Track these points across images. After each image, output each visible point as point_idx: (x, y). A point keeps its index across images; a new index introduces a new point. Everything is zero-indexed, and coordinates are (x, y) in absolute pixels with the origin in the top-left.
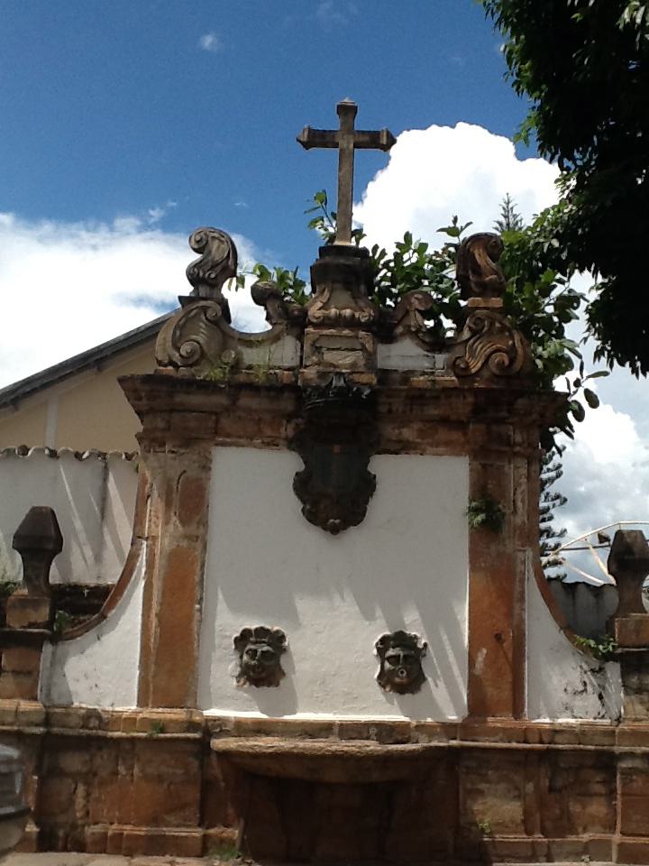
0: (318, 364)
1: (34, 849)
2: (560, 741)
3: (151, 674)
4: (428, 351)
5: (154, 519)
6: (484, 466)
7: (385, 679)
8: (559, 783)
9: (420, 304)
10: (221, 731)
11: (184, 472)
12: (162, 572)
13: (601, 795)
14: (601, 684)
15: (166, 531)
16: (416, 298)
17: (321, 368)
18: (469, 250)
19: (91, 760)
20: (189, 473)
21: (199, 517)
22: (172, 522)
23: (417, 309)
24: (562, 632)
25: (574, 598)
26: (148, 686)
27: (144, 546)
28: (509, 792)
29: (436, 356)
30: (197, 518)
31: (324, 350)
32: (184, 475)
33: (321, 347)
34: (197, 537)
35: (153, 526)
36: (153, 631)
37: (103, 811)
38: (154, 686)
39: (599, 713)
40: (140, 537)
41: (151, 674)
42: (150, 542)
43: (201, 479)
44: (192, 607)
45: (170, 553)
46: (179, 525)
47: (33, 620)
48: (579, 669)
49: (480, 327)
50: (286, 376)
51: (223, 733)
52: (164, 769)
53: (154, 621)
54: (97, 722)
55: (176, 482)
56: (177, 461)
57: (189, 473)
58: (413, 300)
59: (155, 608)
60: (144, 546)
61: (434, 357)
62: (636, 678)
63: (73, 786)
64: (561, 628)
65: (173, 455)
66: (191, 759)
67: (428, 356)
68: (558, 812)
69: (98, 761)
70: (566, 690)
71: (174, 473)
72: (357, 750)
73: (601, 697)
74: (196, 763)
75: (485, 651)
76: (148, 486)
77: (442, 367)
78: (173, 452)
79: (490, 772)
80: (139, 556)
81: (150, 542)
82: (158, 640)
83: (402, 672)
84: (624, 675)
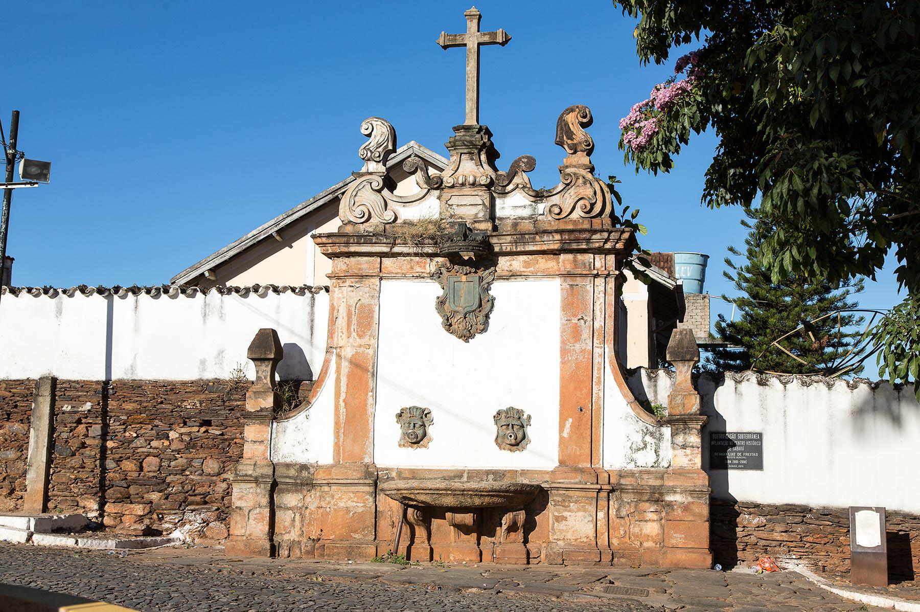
2: (624, 483)
3: (341, 440)
5: (340, 334)
7: (499, 441)
8: (624, 513)
10: (388, 478)
16: (523, 162)
20: (363, 301)
24: (629, 405)
30: (369, 333)
31: (454, 207)
32: (360, 302)
34: (369, 345)
35: (340, 338)
36: (341, 411)
41: (341, 440)
42: (338, 350)
48: (641, 432)
49: (569, 181)
50: (432, 229)
52: (350, 504)
53: (342, 404)
56: (354, 293)
57: (363, 301)
59: (343, 396)
62: (682, 437)
63: (293, 515)
65: (352, 288)
66: (368, 497)
68: (622, 532)
69: (308, 499)
74: (371, 500)
75: (571, 420)
76: (336, 311)
79: (572, 504)
82: (345, 417)
83: (511, 436)
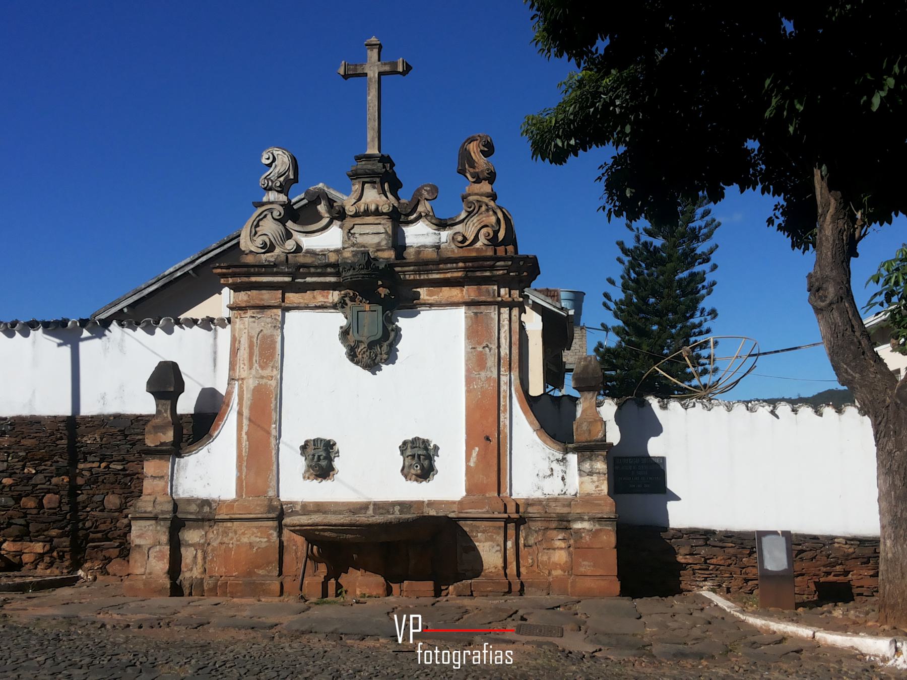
0: (354, 245)
1: (169, 594)
2: (531, 511)
3: (244, 474)
4: (435, 230)
5: (242, 366)
6: (476, 314)
7: (405, 472)
8: (531, 541)
9: (428, 194)
10: (292, 511)
11: (262, 330)
12: (249, 403)
13: (562, 549)
14: (564, 469)
15: (250, 373)
16: (425, 190)
17: (355, 249)
18: (466, 149)
19: (206, 534)
20: (265, 332)
21: (272, 363)
22: (254, 367)
23: (426, 199)
24: (535, 433)
25: (559, 408)
26: (242, 485)
27: (237, 384)
28: (493, 547)
29: (441, 233)
30: (271, 364)
31: (357, 236)
32: (262, 333)
33: (355, 233)
34: (272, 377)
35: (242, 370)
36: (244, 444)
37: (215, 569)
38: (246, 483)
39: (562, 491)
40: (233, 379)
41: (244, 474)
42: (240, 382)
43: (274, 335)
44: (270, 426)
45: (253, 389)
46: (259, 369)
47: (162, 441)
48: (548, 459)
49: (471, 209)
50: (333, 258)
51: (294, 513)
52: (253, 539)
53: (245, 437)
54: (208, 509)
55: (256, 339)
56: (256, 324)
57: (265, 332)
58: (424, 192)
59: (245, 428)
60: (237, 384)
61: (440, 234)
62: (588, 464)
63: (195, 552)
64: (535, 430)
65: (254, 319)
66: (271, 531)
67: (435, 234)
68: (530, 561)
69: (210, 535)
70: (538, 475)
71: (254, 333)
72: (366, 519)
73: (563, 479)
74: (275, 534)
75: (477, 449)
76: (237, 342)
77: (445, 241)
78: (254, 317)
79: (479, 534)
80: (233, 392)
81: (240, 382)
82: (247, 450)
83: (417, 467)
84: (579, 462)
